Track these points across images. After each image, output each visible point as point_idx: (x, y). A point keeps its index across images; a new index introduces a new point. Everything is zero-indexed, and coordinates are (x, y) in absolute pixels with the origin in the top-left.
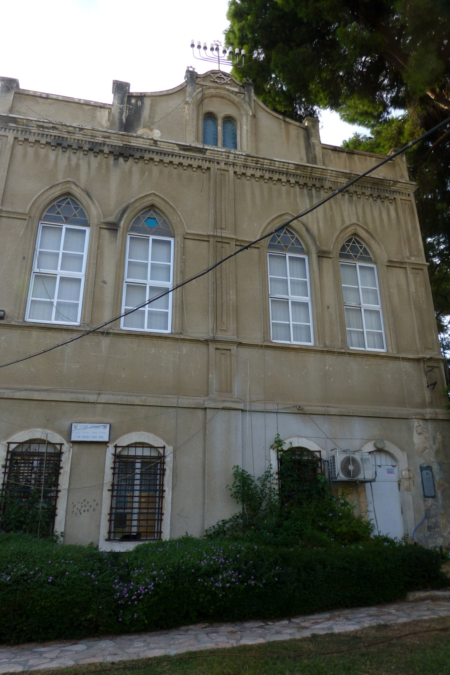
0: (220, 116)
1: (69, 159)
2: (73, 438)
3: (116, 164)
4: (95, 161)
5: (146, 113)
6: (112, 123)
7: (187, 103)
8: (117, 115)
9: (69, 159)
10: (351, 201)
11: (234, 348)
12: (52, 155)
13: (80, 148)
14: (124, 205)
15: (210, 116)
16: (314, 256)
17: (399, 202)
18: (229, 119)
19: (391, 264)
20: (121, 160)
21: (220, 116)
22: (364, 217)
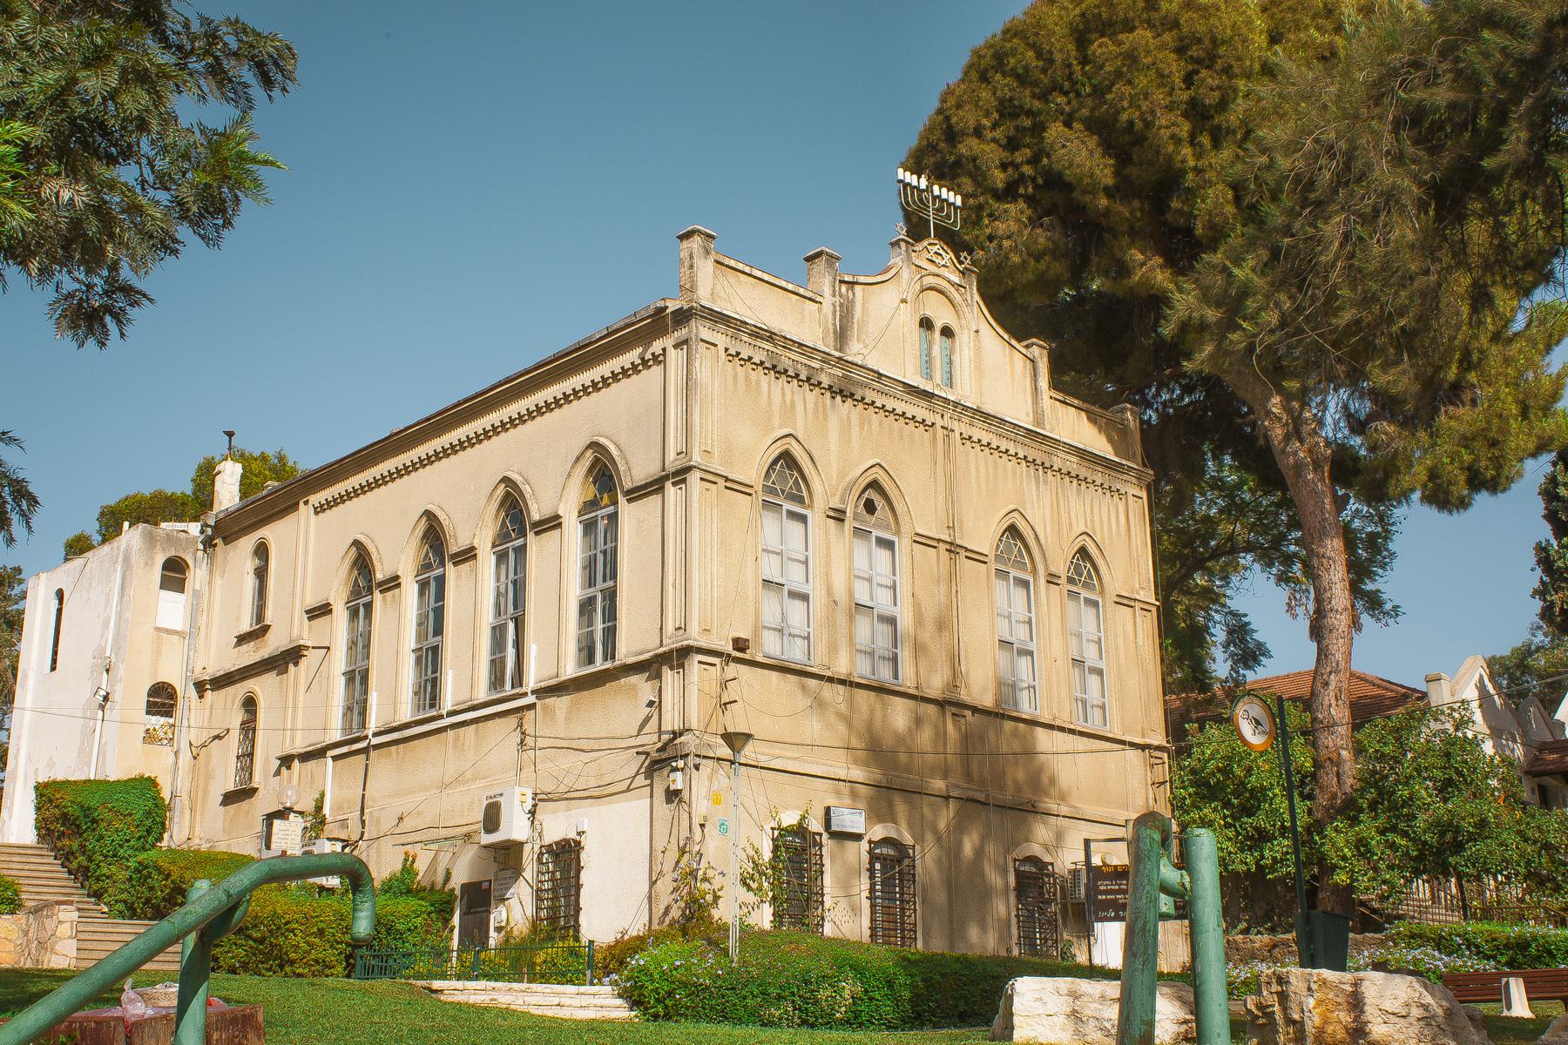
0: (938, 325)
1: (783, 394)
2: (834, 828)
3: (833, 406)
4: (812, 396)
5: (858, 313)
6: (826, 331)
7: (904, 301)
8: (830, 316)
9: (783, 394)
10: (1079, 492)
11: (968, 713)
12: (764, 380)
13: (797, 375)
14: (847, 479)
15: (926, 324)
16: (1042, 581)
17: (1131, 498)
18: (947, 332)
19: (1124, 601)
20: (839, 398)
21: (938, 325)
22: (1093, 521)
